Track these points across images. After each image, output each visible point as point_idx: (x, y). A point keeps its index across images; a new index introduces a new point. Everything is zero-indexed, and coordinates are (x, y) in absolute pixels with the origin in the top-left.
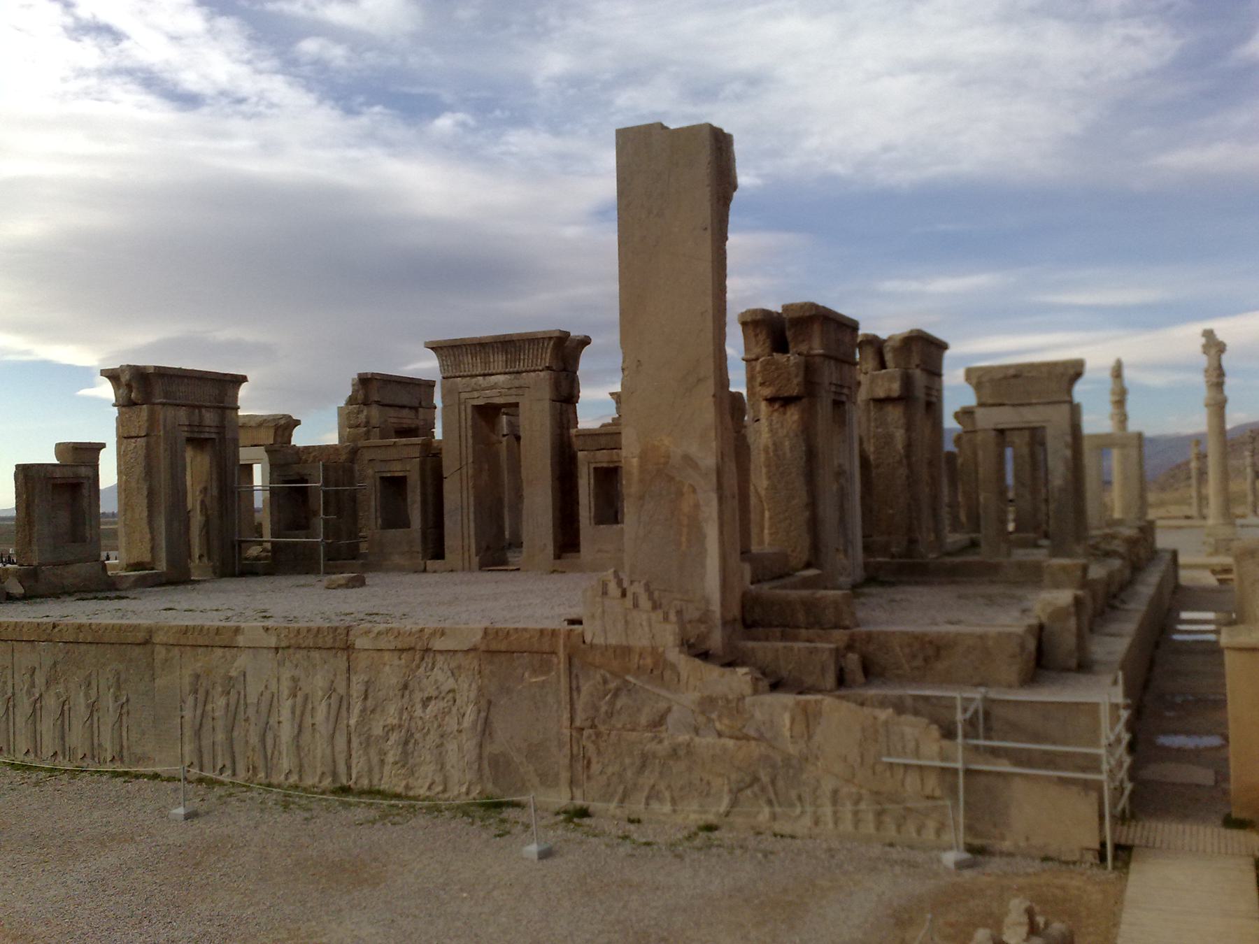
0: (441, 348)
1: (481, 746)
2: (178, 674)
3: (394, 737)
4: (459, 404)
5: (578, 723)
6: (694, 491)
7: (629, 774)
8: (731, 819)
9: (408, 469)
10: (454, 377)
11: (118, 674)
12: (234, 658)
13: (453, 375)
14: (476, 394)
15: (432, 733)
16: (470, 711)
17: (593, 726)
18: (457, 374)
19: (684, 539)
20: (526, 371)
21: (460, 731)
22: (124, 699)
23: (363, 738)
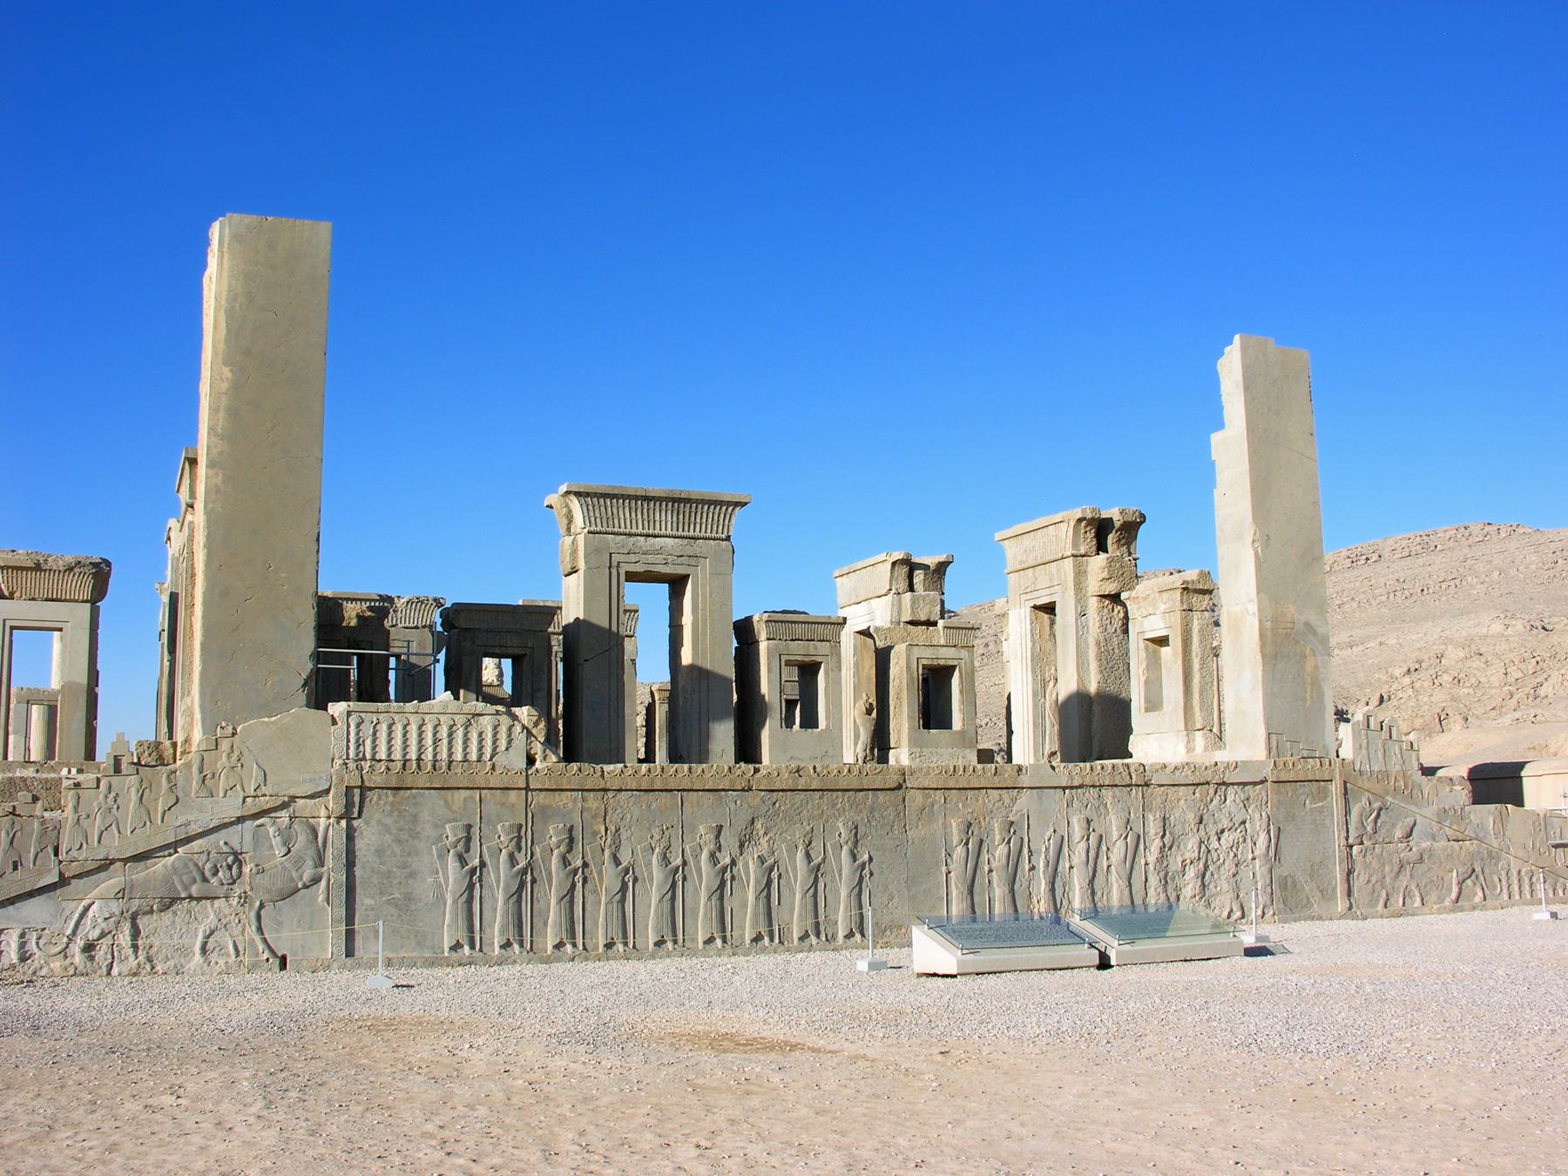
0: (587, 494)
1: (1271, 871)
2: (940, 823)
3: (1191, 872)
4: (610, 567)
5: (1351, 841)
6: (1314, 655)
7: (1388, 880)
8: (1460, 904)
9: (530, 645)
10: (604, 533)
11: (856, 827)
12: (1013, 801)
13: (603, 530)
14: (633, 558)
15: (1226, 864)
16: (1262, 840)
17: (1362, 843)
18: (610, 530)
19: (1308, 696)
20: (703, 538)
21: (1254, 859)
22: (866, 857)
23: (1162, 874)
